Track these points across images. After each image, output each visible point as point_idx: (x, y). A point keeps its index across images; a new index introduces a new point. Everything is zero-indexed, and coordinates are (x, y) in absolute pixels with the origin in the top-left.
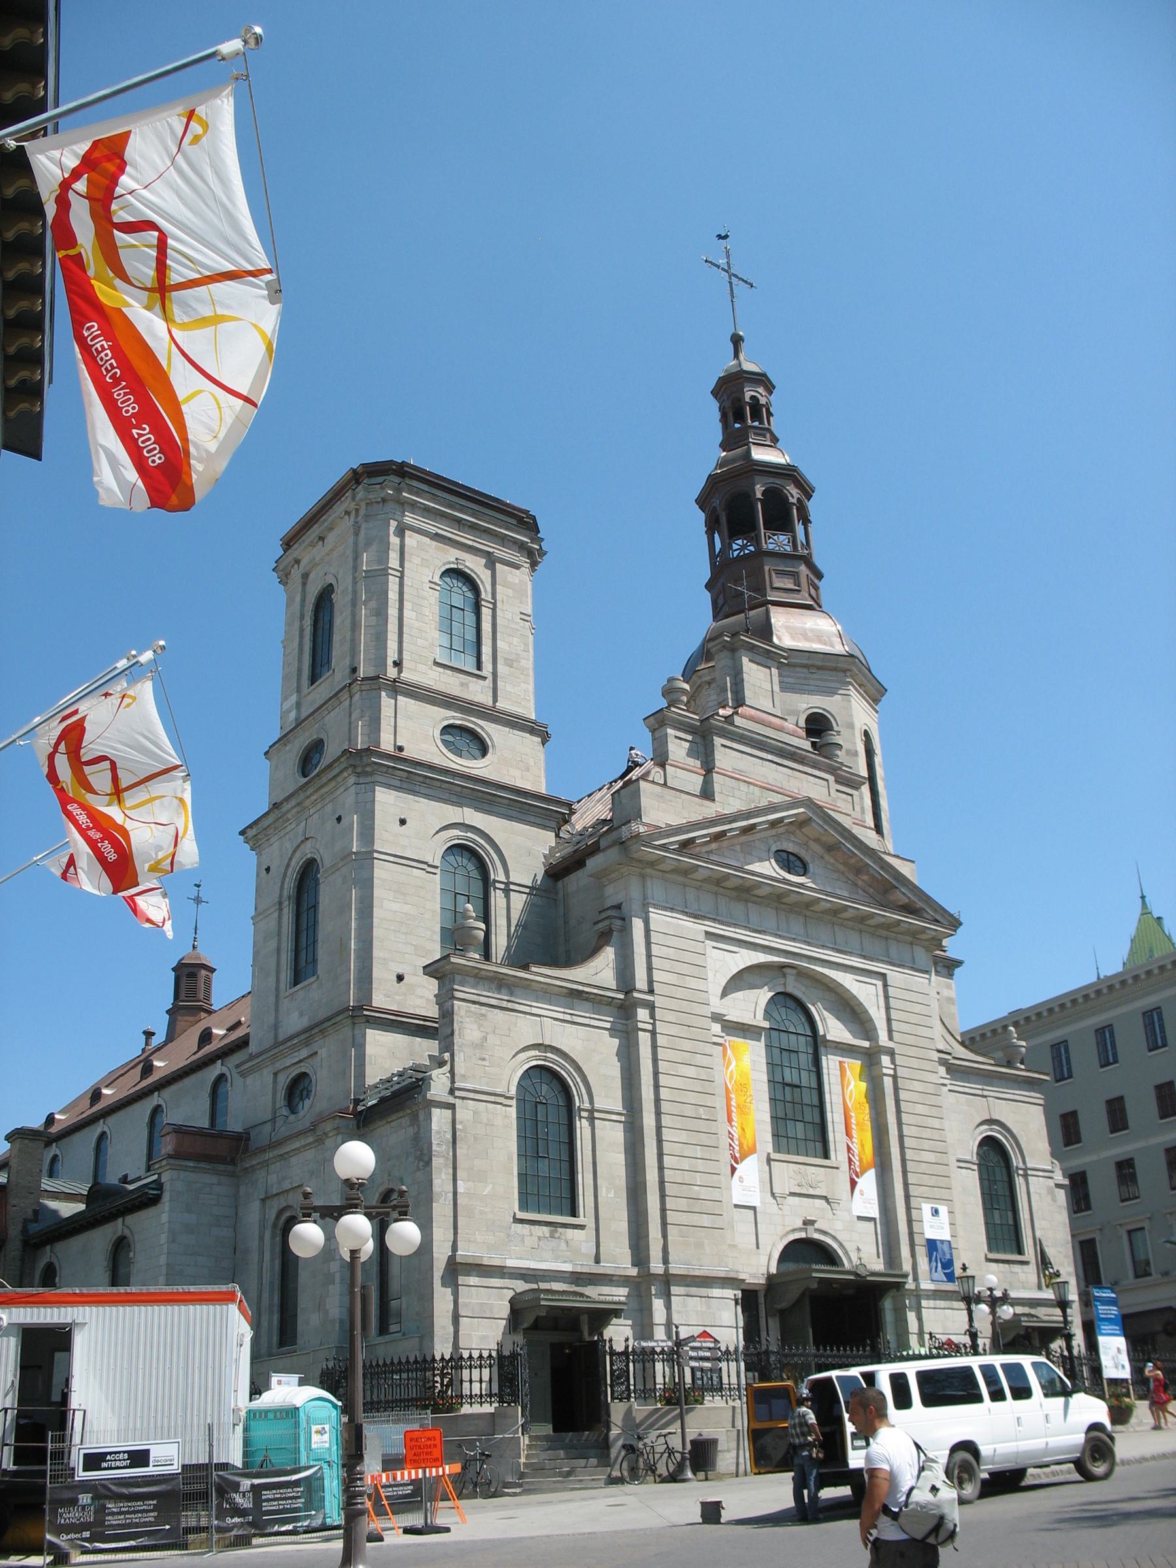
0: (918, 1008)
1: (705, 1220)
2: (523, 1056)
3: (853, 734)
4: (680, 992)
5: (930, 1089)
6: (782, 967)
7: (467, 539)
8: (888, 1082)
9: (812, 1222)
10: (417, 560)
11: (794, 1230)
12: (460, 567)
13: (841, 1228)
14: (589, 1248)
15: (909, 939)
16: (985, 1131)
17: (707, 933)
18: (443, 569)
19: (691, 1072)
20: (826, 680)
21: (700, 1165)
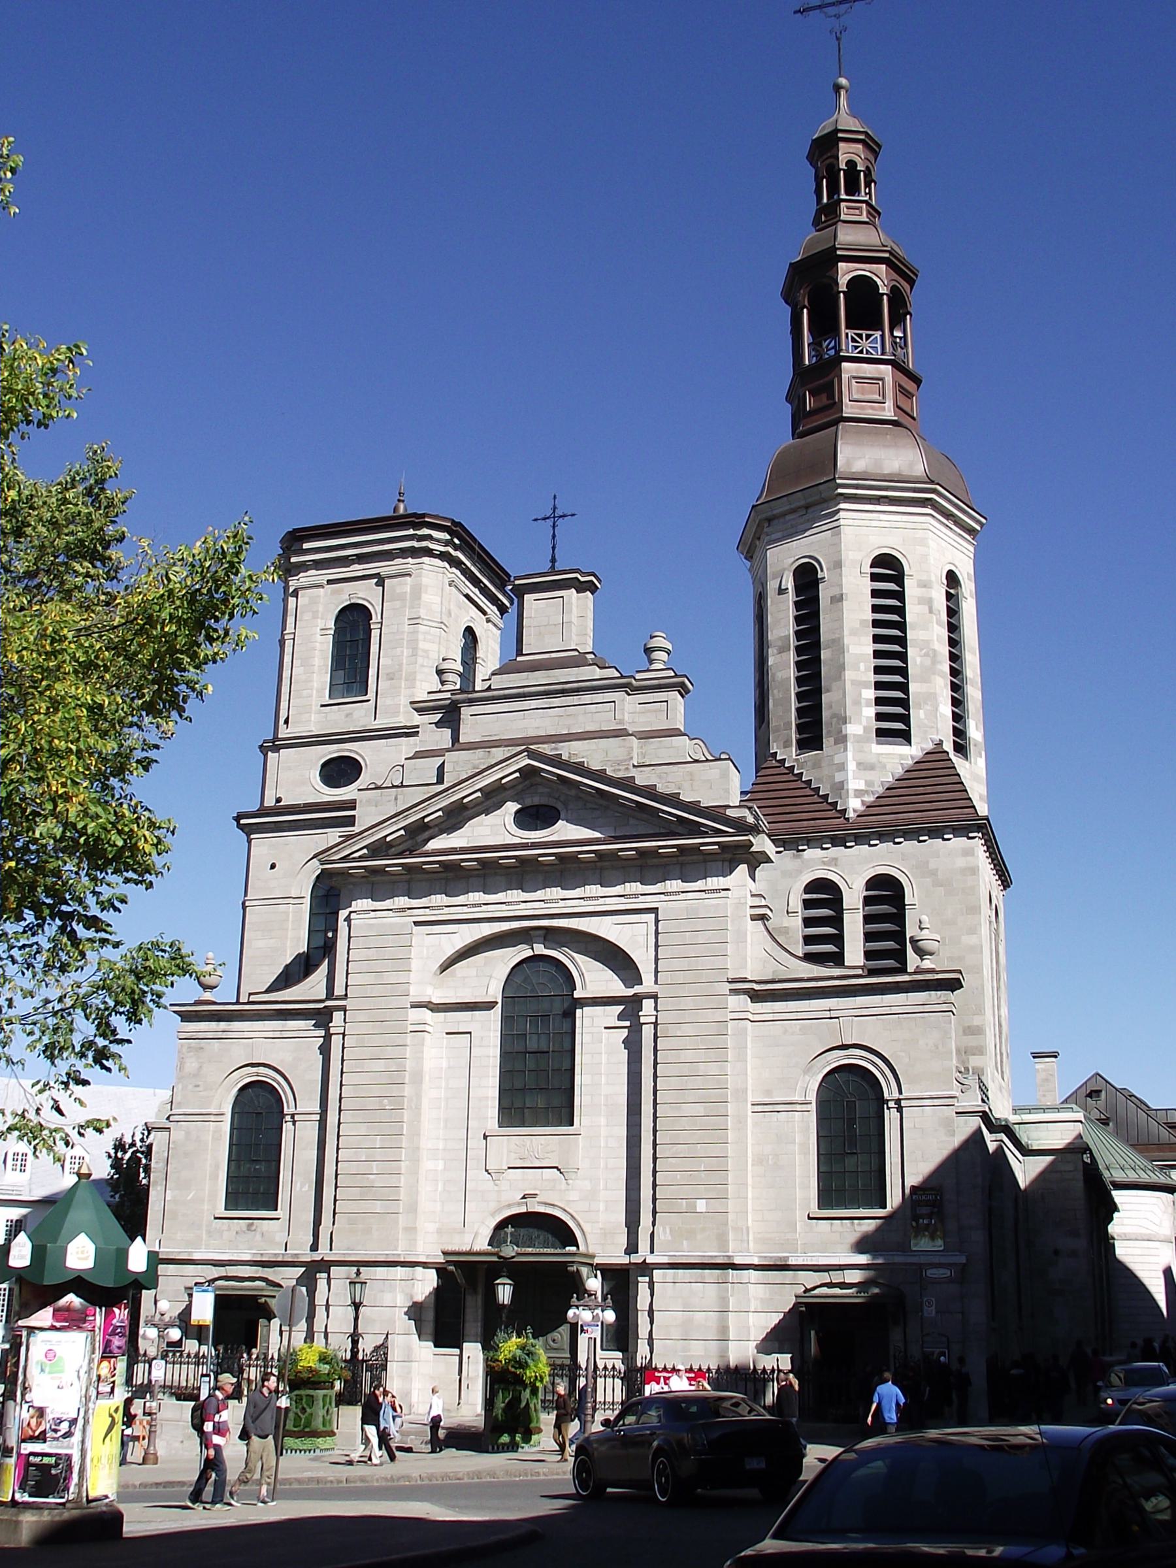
0: (701, 937)
1: (378, 1207)
3: (841, 575)
4: (377, 990)
5: (712, 1029)
8: (647, 1032)
14: (281, 1237)
15: (701, 857)
16: (838, 1059)
19: (380, 1065)
21: (378, 1154)
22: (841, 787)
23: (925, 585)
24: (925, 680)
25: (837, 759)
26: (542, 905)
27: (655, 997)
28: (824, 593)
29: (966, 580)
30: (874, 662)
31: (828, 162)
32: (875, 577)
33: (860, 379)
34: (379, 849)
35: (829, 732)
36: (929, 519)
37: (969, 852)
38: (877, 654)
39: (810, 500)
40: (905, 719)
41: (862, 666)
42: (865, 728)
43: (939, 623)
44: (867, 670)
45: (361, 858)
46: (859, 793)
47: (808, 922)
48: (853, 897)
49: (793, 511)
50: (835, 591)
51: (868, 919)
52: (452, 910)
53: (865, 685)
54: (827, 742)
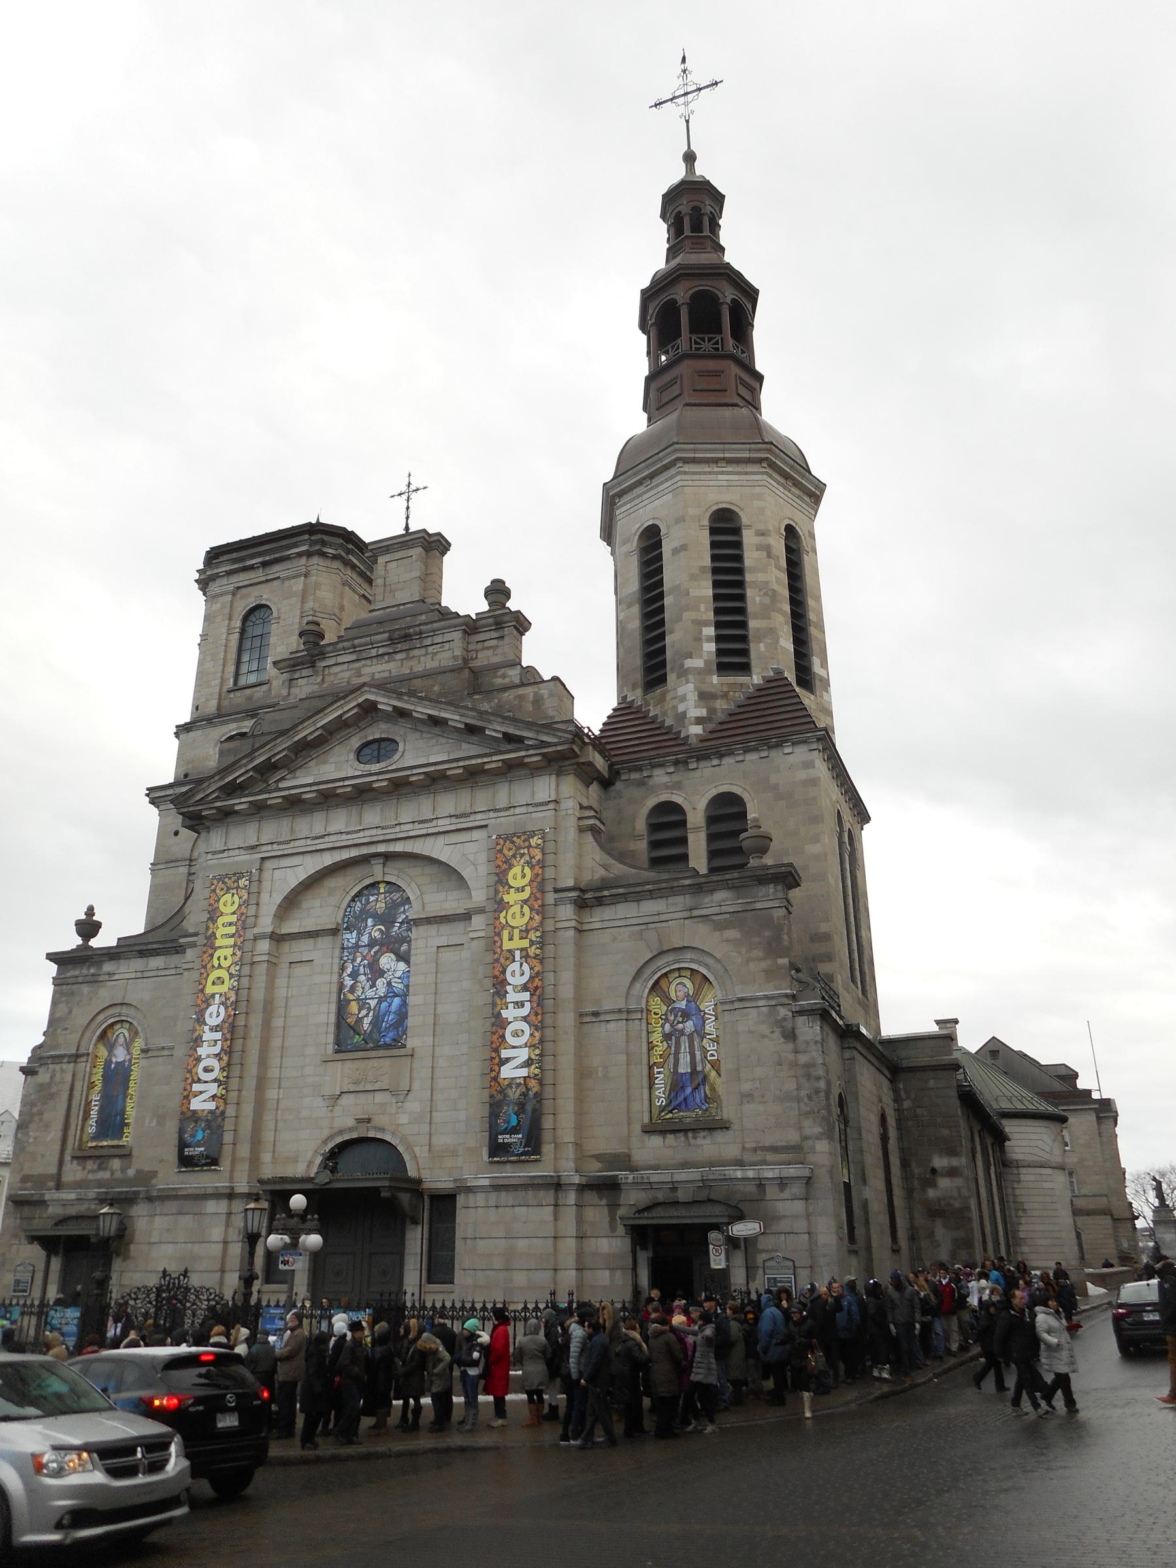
2: (101, 1017)
6: (365, 860)
7: (258, 575)
9: (369, 1120)
10: (218, 619)
11: (341, 1132)
12: (257, 603)
13: (406, 1121)
17: (263, 859)
20: (657, 486)
22: (684, 713)
23: (762, 534)
25: (681, 691)
26: (380, 832)
27: (481, 911)
28: (667, 549)
29: (807, 538)
30: (711, 605)
32: (713, 531)
33: (702, 374)
34: (232, 789)
35: (672, 669)
36: (765, 477)
37: (809, 765)
38: (717, 597)
40: (745, 653)
41: (702, 607)
42: (705, 661)
43: (778, 567)
44: (707, 610)
45: (217, 799)
46: (699, 721)
47: (654, 845)
49: (639, 483)
50: (676, 544)
51: (711, 838)
52: (297, 843)
53: (706, 624)
54: (671, 677)
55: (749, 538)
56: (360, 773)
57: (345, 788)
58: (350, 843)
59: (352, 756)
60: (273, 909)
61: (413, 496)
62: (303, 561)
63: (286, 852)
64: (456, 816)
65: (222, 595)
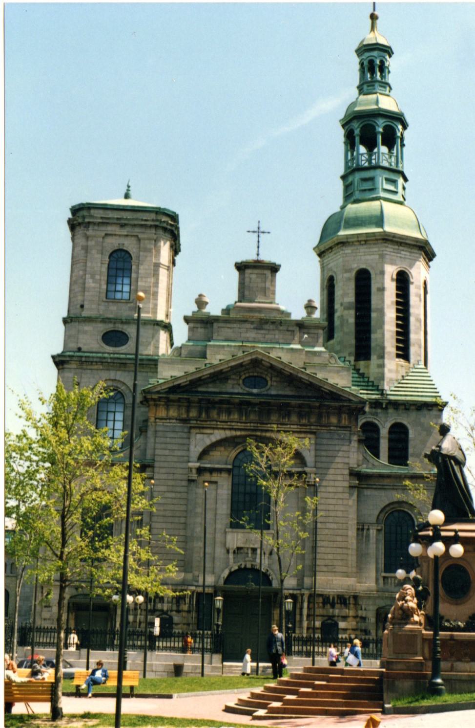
3: (383, 278)
12: (121, 247)
18: (111, 251)
24: (417, 333)
31: (370, 58)
39: (368, 239)
48: (384, 432)
50: (379, 285)
55: (413, 289)
56: (245, 392)
57: (237, 399)
58: (243, 427)
59: (241, 382)
60: (197, 454)
61: (261, 235)
62: (153, 231)
63: (205, 426)
64: (301, 425)
65: (95, 236)
